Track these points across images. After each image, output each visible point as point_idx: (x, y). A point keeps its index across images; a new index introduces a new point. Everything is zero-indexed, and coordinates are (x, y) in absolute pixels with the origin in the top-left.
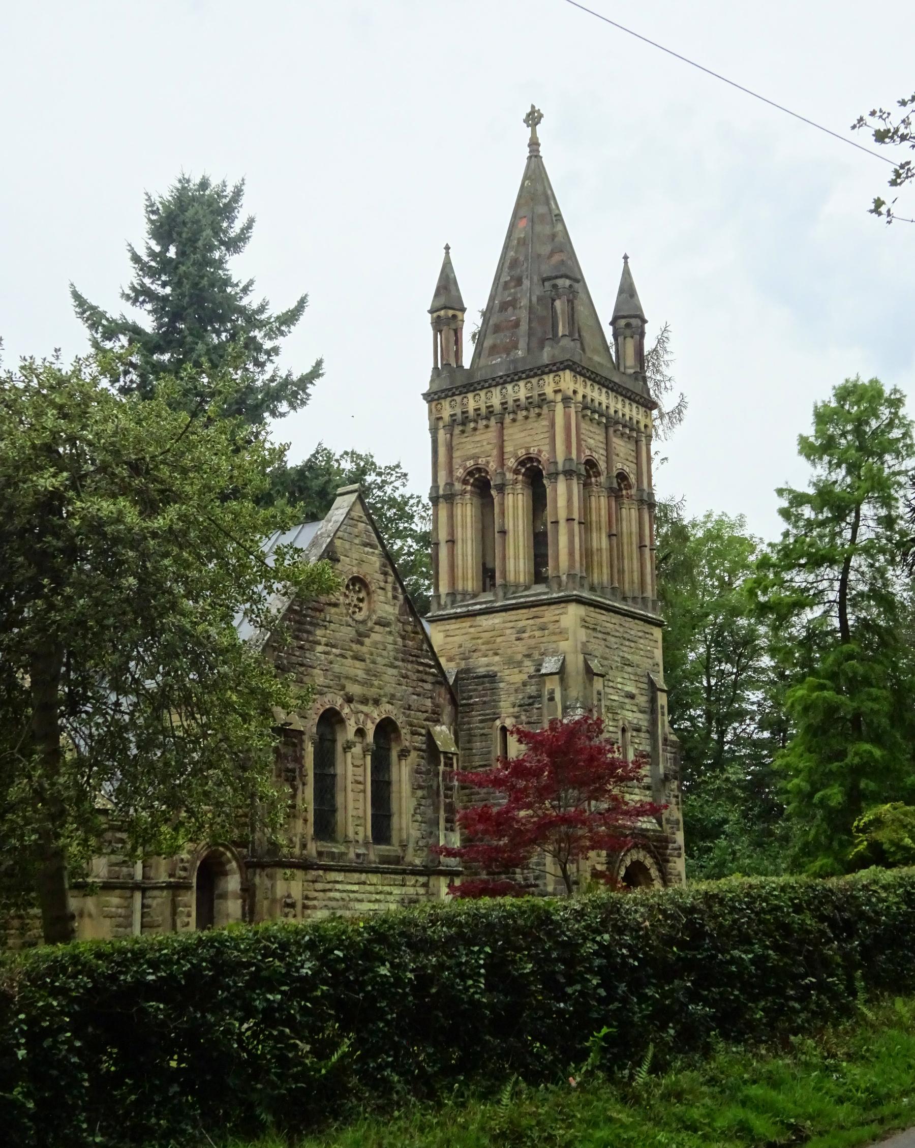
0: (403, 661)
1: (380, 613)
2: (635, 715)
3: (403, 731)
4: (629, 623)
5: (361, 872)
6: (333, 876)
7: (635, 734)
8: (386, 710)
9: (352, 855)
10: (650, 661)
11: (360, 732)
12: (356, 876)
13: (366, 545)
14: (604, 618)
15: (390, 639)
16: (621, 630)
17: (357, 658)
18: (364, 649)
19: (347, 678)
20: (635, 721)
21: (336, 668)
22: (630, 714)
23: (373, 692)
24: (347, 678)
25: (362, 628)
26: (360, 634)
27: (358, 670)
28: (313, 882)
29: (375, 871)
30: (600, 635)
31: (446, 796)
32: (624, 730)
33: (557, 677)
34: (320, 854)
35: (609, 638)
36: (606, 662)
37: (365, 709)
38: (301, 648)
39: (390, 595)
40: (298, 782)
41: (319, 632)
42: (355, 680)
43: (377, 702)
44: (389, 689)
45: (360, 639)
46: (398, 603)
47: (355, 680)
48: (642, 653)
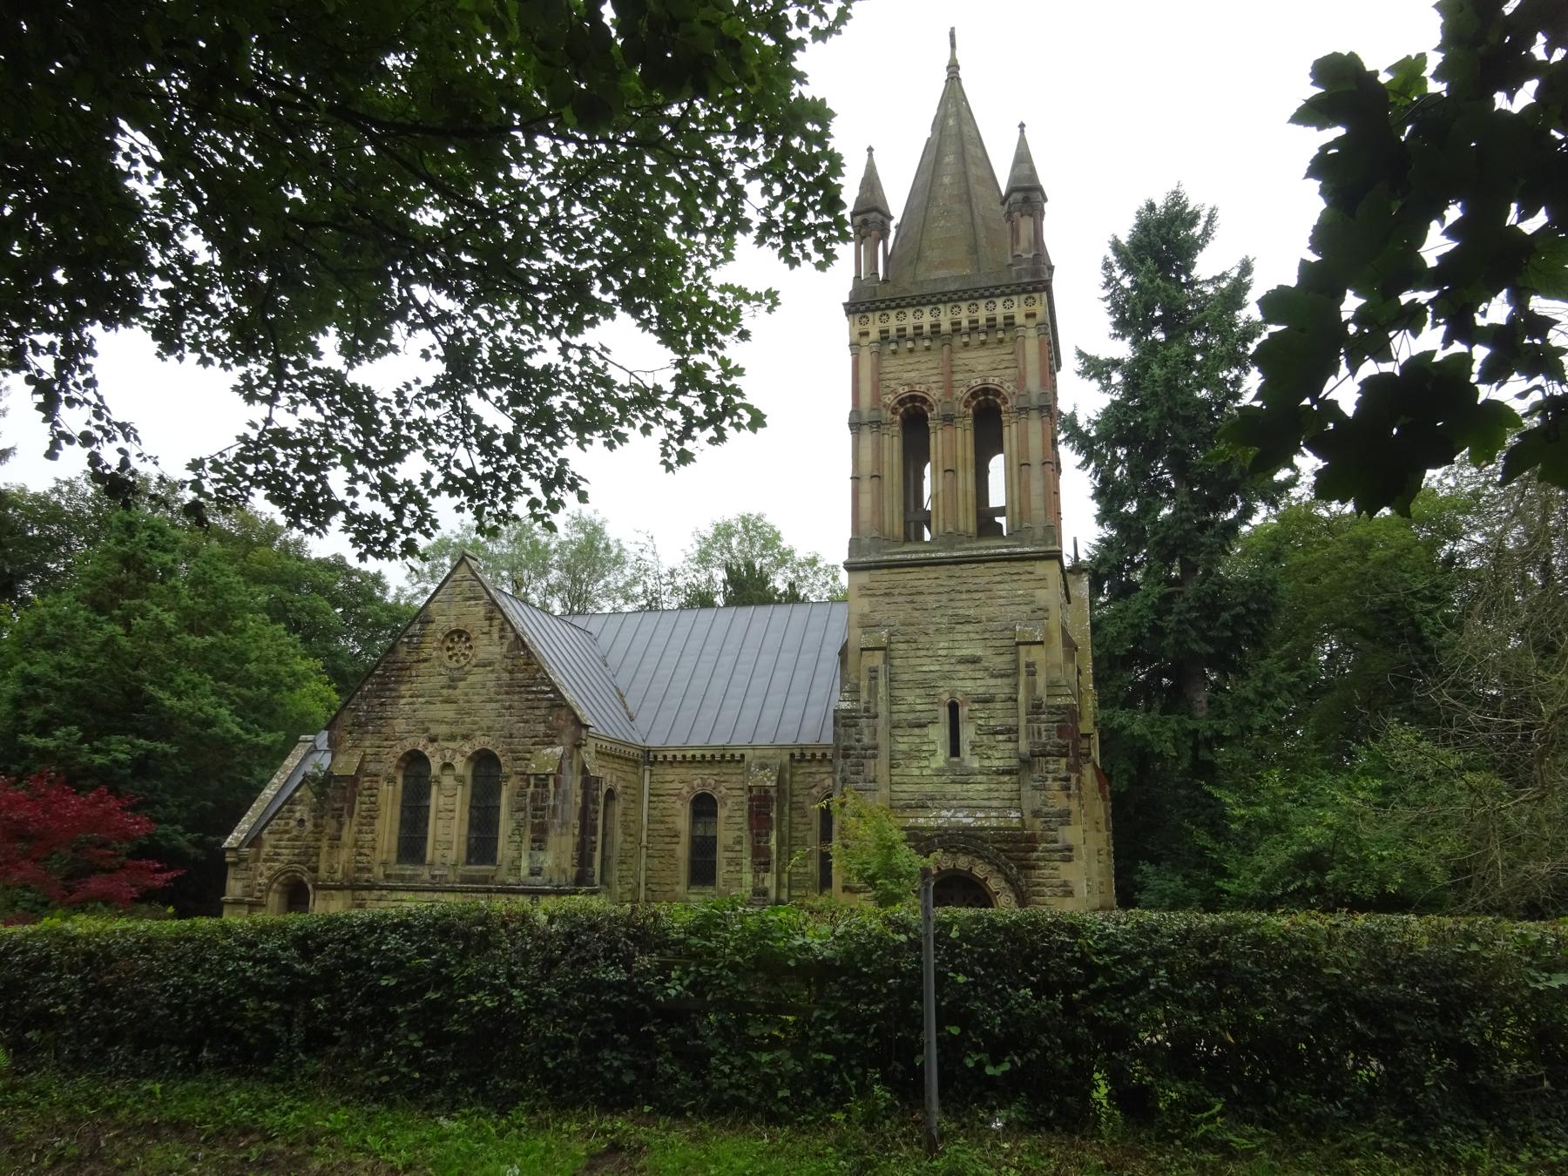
0: (507, 693)
1: (481, 655)
2: (979, 682)
3: (502, 760)
5: (435, 891)
6: (400, 895)
7: (976, 706)
8: (481, 742)
9: (426, 876)
10: (1027, 608)
11: (447, 766)
12: (427, 895)
13: (469, 599)
14: (909, 576)
15: (493, 676)
16: (953, 582)
17: (447, 701)
18: (458, 692)
19: (431, 721)
20: (981, 690)
21: (421, 714)
22: (969, 683)
23: (463, 729)
24: (431, 721)
25: (456, 674)
27: (449, 712)
28: (379, 900)
29: (453, 890)
30: (901, 599)
31: (534, 817)
32: (954, 708)
33: (880, 654)
34: (388, 877)
35: (916, 598)
37: (452, 745)
38: (382, 704)
39: (496, 636)
41: (403, 687)
43: (466, 737)
45: (452, 683)
46: (506, 642)
48: (1002, 601)
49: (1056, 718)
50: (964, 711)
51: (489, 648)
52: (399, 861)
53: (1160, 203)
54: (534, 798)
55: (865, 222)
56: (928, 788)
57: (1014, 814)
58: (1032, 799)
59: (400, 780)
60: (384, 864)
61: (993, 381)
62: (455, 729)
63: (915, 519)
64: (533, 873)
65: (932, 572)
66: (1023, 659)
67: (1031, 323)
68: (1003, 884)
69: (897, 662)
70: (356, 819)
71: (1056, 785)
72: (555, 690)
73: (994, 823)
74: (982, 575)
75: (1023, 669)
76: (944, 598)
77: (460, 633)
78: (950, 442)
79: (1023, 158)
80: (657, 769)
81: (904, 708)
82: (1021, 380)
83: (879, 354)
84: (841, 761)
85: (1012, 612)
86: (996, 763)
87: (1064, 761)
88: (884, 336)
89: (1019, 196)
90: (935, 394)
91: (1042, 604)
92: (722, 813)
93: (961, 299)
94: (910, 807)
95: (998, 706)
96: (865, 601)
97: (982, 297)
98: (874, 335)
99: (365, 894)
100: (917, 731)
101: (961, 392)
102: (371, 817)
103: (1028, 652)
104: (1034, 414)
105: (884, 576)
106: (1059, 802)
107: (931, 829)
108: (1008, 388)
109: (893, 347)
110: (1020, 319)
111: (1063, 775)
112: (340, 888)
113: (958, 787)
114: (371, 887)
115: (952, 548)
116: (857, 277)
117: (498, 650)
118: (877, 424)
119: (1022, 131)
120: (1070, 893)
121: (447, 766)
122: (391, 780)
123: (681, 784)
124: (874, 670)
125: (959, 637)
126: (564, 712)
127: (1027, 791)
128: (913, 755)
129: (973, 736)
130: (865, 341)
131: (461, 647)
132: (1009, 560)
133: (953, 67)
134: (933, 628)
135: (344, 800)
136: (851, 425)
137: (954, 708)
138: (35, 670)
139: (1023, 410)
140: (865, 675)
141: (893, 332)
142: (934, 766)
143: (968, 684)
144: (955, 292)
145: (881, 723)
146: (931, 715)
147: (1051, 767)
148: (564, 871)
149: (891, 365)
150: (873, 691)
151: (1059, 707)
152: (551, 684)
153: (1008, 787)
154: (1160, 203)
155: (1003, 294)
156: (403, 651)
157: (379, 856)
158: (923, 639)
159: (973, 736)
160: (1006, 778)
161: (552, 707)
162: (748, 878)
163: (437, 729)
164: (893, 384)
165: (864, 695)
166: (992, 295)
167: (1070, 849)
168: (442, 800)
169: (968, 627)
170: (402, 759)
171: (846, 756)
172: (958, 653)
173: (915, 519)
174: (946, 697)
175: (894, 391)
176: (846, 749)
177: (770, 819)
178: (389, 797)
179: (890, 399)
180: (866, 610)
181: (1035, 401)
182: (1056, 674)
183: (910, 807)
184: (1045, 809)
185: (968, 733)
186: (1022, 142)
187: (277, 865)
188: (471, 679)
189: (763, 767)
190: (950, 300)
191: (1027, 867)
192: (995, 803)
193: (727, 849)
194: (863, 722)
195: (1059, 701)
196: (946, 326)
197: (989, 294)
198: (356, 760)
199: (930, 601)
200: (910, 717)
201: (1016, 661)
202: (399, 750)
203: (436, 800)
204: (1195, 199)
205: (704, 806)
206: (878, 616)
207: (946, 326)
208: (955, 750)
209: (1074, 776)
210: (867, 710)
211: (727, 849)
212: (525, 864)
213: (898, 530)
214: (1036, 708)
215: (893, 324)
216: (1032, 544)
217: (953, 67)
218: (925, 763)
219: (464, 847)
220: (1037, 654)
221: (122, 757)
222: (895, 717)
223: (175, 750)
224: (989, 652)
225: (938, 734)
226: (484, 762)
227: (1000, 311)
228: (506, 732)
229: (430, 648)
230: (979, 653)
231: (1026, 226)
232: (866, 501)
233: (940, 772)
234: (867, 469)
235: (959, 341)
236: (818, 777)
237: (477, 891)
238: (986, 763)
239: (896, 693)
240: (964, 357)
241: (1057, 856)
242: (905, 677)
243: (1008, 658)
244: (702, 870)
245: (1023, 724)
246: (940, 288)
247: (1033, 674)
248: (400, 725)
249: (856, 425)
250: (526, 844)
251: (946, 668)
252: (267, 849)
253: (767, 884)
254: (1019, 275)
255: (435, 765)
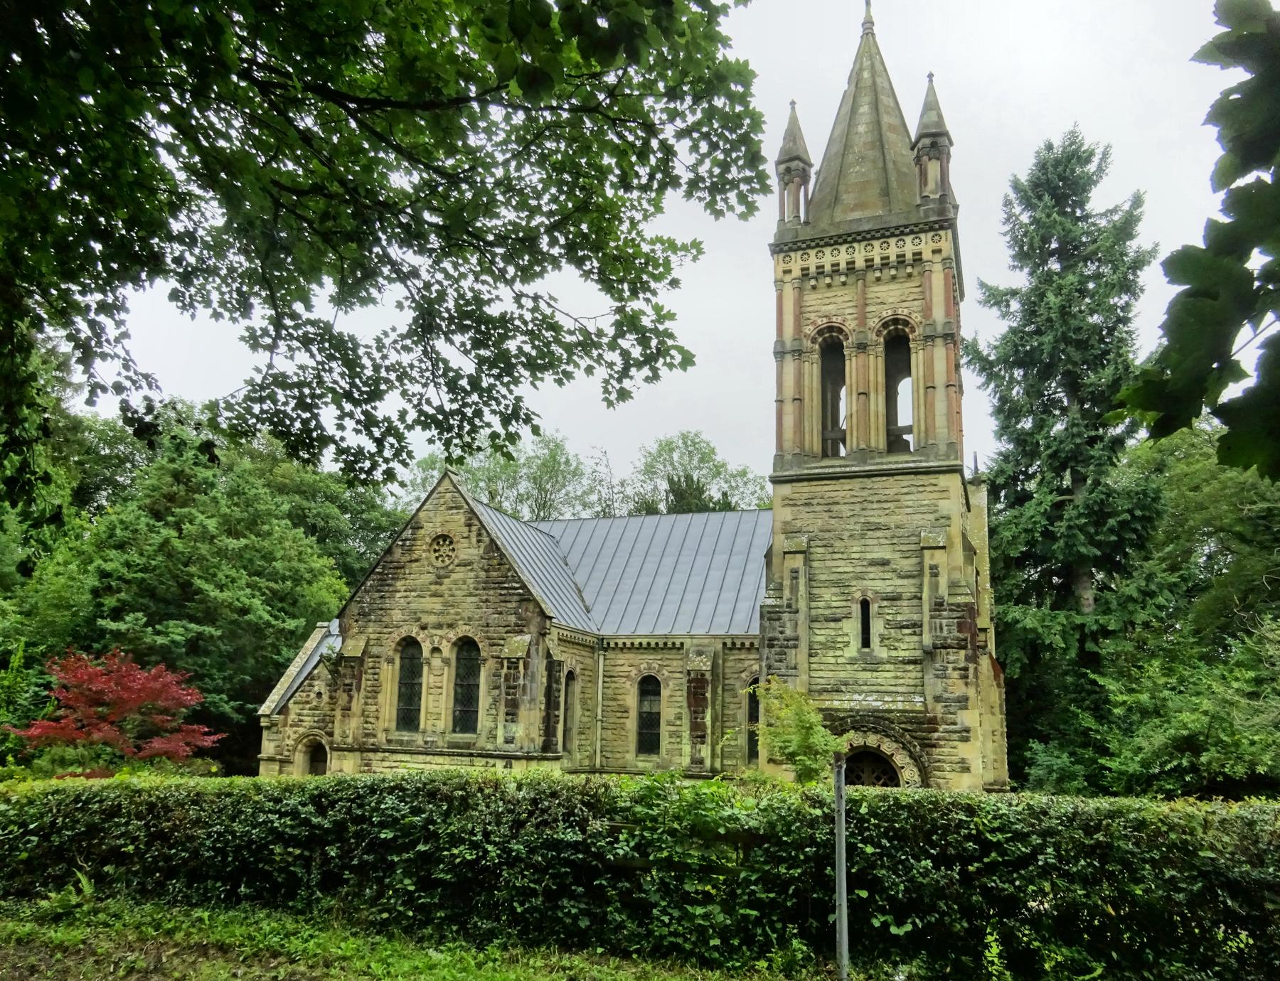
1: (462, 557)
4: (878, 483)
7: (885, 603)
8: (463, 630)
9: (420, 742)
10: (931, 517)
11: (436, 650)
12: (421, 758)
16: (865, 493)
17: (435, 595)
21: (413, 606)
23: (448, 619)
25: (442, 572)
26: (439, 577)
27: (436, 605)
29: (441, 754)
30: (818, 508)
32: (865, 605)
33: (800, 557)
35: (835, 508)
36: (827, 535)
37: (439, 632)
39: (474, 540)
40: (354, 693)
42: (431, 613)
43: (451, 626)
44: (466, 614)
45: (439, 580)
47: (431, 613)
49: (956, 614)
50: (874, 608)
51: (468, 550)
52: (398, 729)
53: (1057, 143)
54: (507, 678)
55: (788, 170)
56: (842, 675)
57: (918, 699)
58: (934, 686)
59: (398, 661)
60: (386, 730)
61: (903, 312)
62: (441, 619)
63: (832, 438)
64: (509, 741)
65: (847, 485)
66: (928, 561)
67: (938, 258)
68: (908, 760)
69: (815, 564)
70: (362, 693)
71: (956, 674)
72: (524, 587)
73: (900, 706)
74: (891, 487)
75: (927, 571)
76: (857, 507)
77: (444, 537)
78: (864, 368)
79: (931, 105)
80: (610, 655)
81: (821, 604)
82: (927, 311)
83: (801, 289)
84: (766, 650)
85: (918, 520)
86: (902, 654)
87: (963, 652)
88: (805, 273)
89: (927, 141)
90: (850, 325)
91: (945, 513)
92: (665, 693)
93: (874, 238)
94: (826, 691)
95: (905, 603)
96: (789, 509)
97: (893, 235)
98: (797, 273)
99: (371, 755)
100: (832, 625)
101: (874, 323)
102: (375, 692)
103: (932, 557)
104: (939, 341)
105: (804, 487)
106: (958, 689)
107: (845, 710)
108: (916, 318)
109: (813, 282)
110: (927, 255)
111: (962, 665)
112: (351, 750)
113: (869, 674)
114: (376, 750)
115: (865, 463)
116: (782, 220)
117: (474, 551)
118: (799, 353)
119: (931, 81)
120: (967, 770)
121: (436, 650)
122: (390, 661)
123: (630, 667)
124: (796, 571)
125: (870, 542)
126: (531, 606)
127: (929, 678)
128: (831, 645)
129: (882, 631)
130: (788, 278)
131: (445, 550)
132: (916, 473)
133: (868, 25)
134: (847, 534)
135: (353, 676)
136: (776, 353)
137: (865, 605)
138: (109, 567)
139: (930, 338)
140: (787, 574)
141: (813, 270)
142: (847, 655)
143: (878, 584)
144: (868, 232)
145: (801, 617)
146: (845, 611)
147: (952, 658)
148: (533, 740)
149: (811, 299)
150: (794, 589)
151: (959, 605)
152: (520, 581)
153: (913, 674)
154: (1057, 143)
155: (912, 232)
156: (398, 552)
157: (382, 724)
158: (838, 544)
159: (882, 631)
160: (911, 667)
161: (521, 601)
162: (687, 749)
163: (426, 619)
164: (812, 316)
165: (787, 593)
166: (902, 233)
167: (967, 731)
168: (432, 679)
169: (879, 534)
170: (399, 644)
171: (771, 646)
172: (869, 556)
173: (832, 438)
174: (858, 595)
175: (814, 323)
176: (771, 639)
177: (705, 699)
178: (389, 675)
179: (809, 330)
180: (789, 518)
181: (940, 329)
182: (956, 575)
183: (826, 691)
184: (946, 695)
185: (877, 627)
186: (931, 90)
187: (301, 730)
188: (454, 576)
189: (700, 653)
190: (864, 239)
191: (929, 745)
192: (900, 689)
193: (669, 724)
194: (786, 616)
195: (960, 600)
196: (860, 263)
197: (899, 232)
198: (362, 644)
199: (845, 510)
200: (827, 612)
201: (921, 564)
202: (397, 636)
203: (427, 679)
204: (1089, 139)
205: (649, 687)
206: (799, 524)
207: (860, 263)
208: (866, 642)
209: (972, 666)
210: (789, 606)
211: (669, 724)
212: (500, 733)
213: (817, 448)
214: (938, 606)
215: (812, 261)
216: (937, 458)
217: (868, 25)
218: (839, 653)
219: (450, 718)
220: (939, 558)
221: (178, 638)
222: (814, 612)
223: (219, 633)
224: (898, 555)
225: (852, 627)
226: (466, 646)
227: (909, 247)
228: (483, 622)
229: (421, 550)
230: (888, 556)
231: (933, 168)
232: (789, 421)
233: (852, 661)
234: (789, 391)
235: (871, 276)
236: (747, 663)
237: (461, 755)
238: (894, 653)
239: (815, 591)
240: (876, 291)
241: (955, 736)
242: (823, 577)
243: (914, 561)
244: (648, 742)
245: (926, 619)
246: (855, 228)
247: (936, 575)
248: (397, 615)
249: (780, 354)
250: (501, 717)
251: (859, 569)
252: (292, 717)
253: (703, 754)
254: (927, 216)
255: (426, 648)
